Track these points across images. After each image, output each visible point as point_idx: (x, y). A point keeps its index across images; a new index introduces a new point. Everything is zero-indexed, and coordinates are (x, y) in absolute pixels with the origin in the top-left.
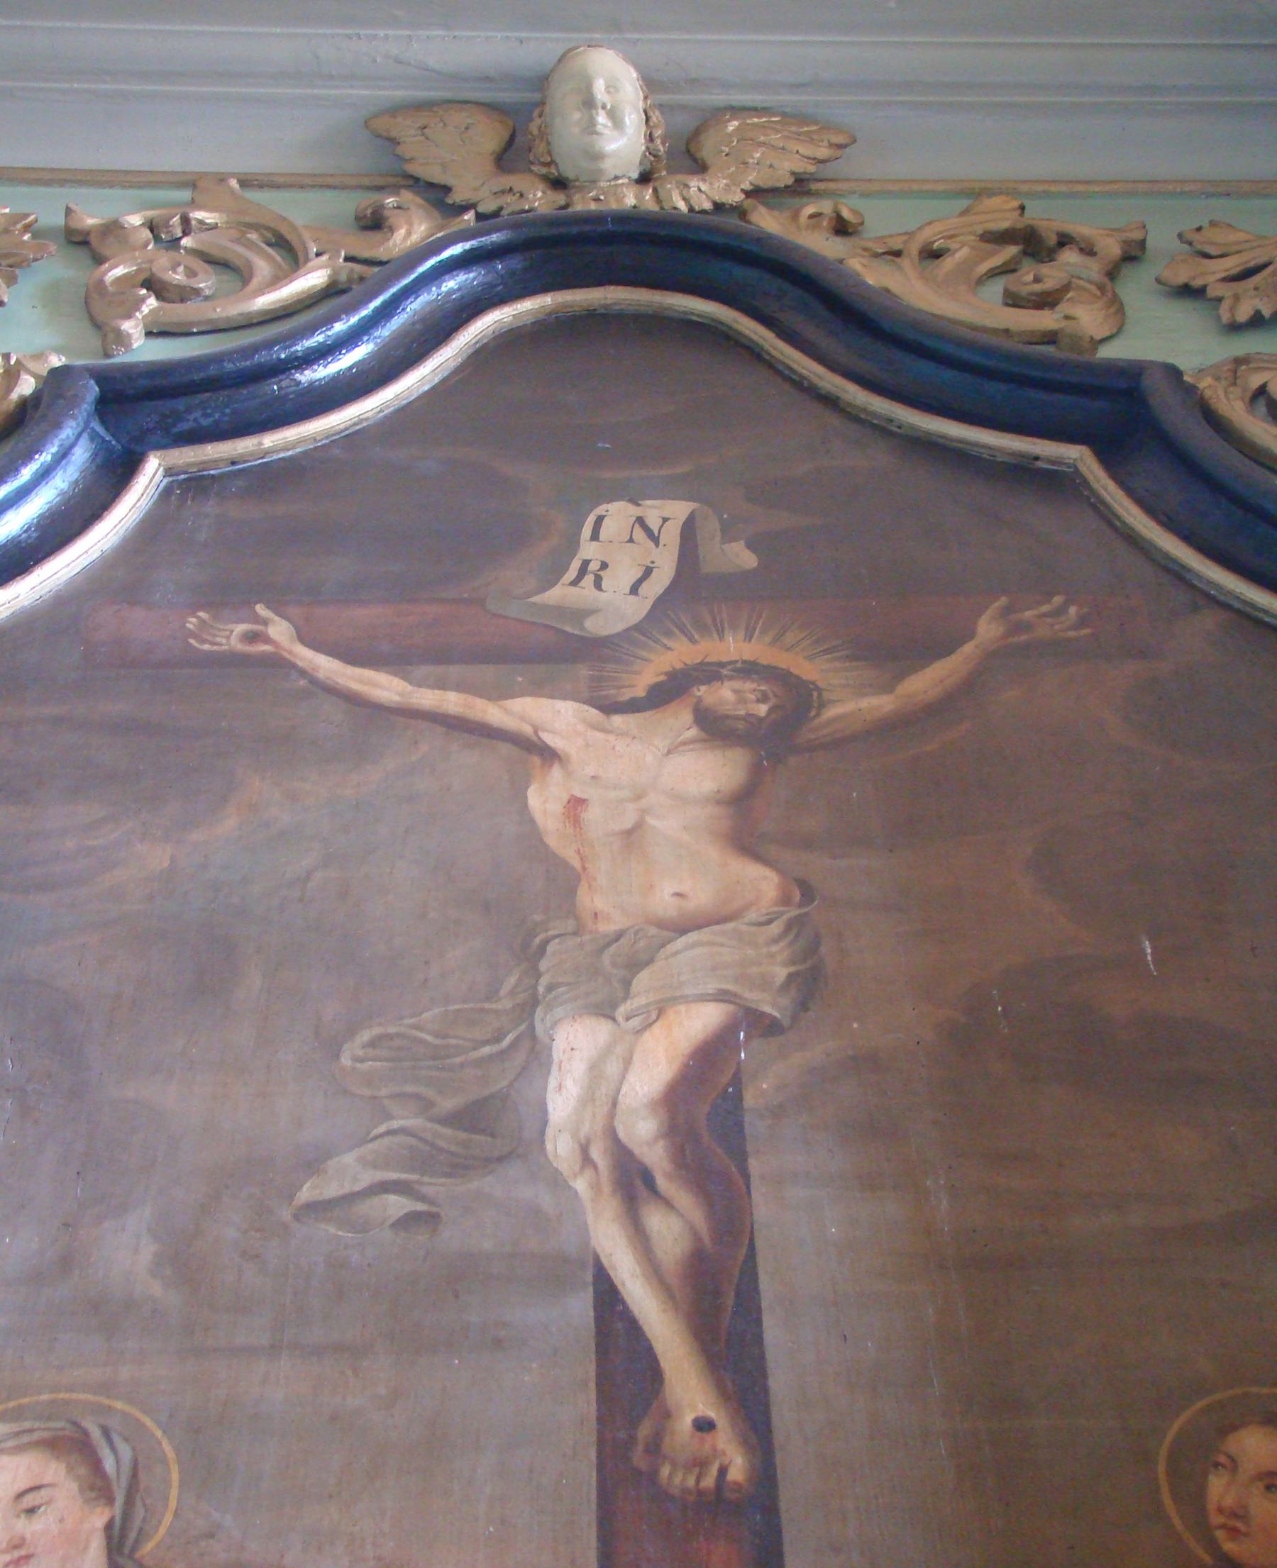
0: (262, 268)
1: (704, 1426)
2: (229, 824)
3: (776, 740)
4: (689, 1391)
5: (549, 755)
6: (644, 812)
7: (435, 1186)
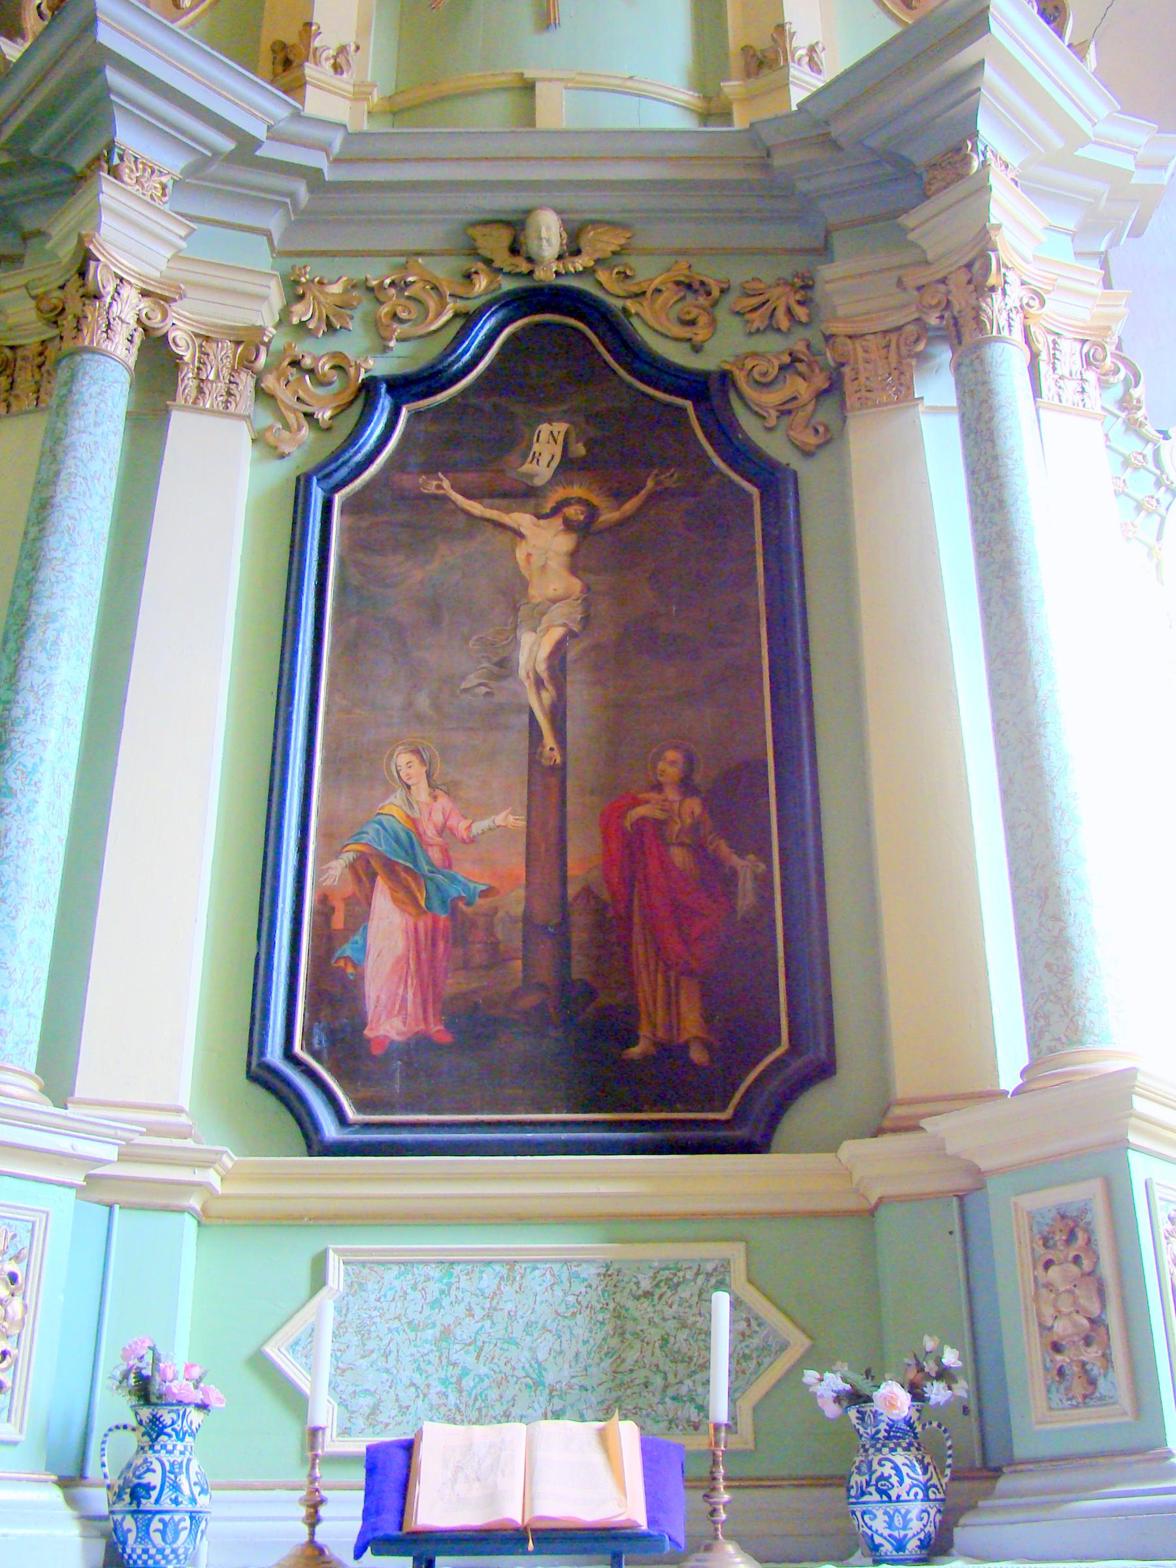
0: (432, 304)
1: (552, 749)
2: (436, 565)
3: (584, 529)
4: (549, 741)
5: (521, 536)
6: (547, 559)
7: (493, 684)
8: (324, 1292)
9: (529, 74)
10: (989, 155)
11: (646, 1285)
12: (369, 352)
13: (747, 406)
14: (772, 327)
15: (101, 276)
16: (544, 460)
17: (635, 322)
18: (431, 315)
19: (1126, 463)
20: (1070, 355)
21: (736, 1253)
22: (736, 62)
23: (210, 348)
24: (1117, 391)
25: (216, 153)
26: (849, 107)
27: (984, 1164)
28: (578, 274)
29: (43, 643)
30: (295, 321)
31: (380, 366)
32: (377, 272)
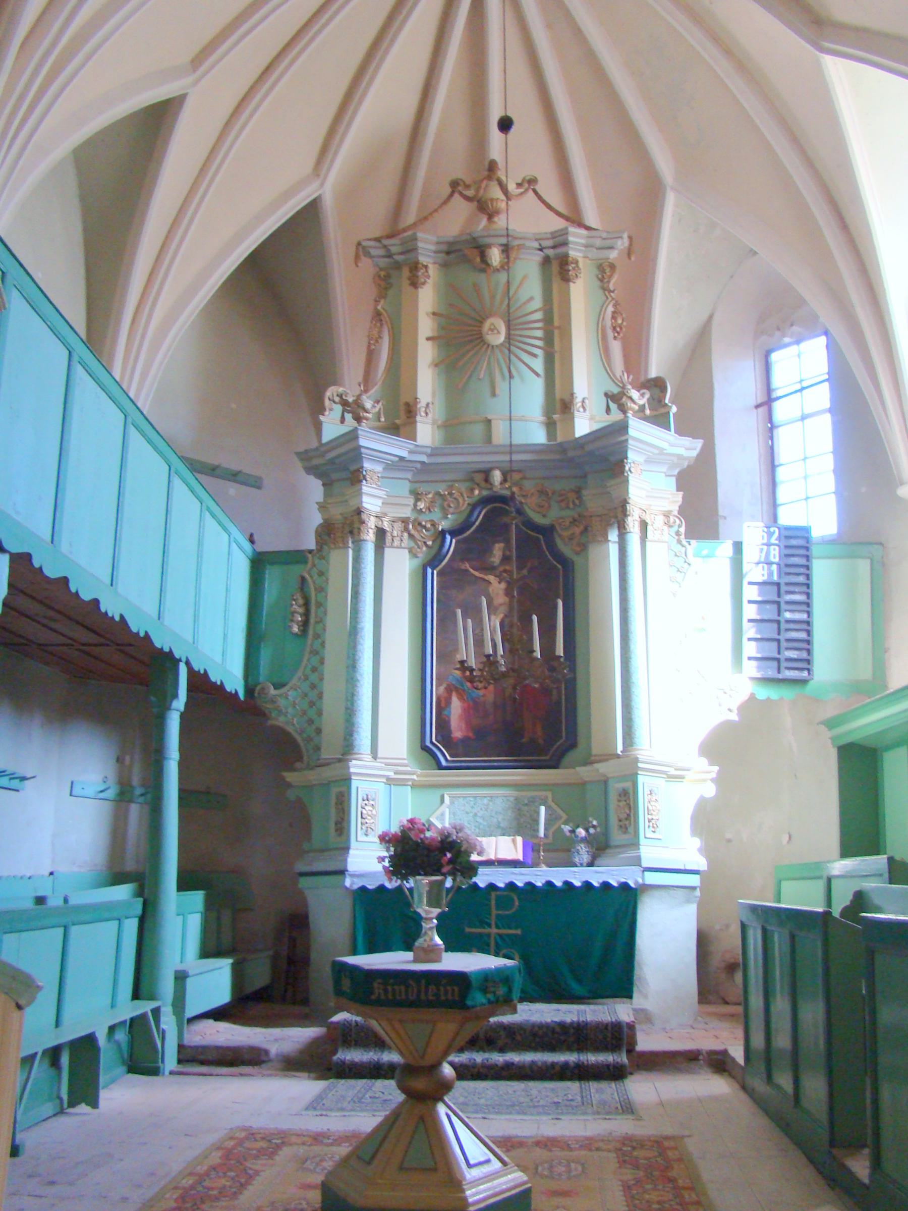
8: (444, 805)
9: (489, 418)
11: (526, 802)
14: (568, 507)
15: (364, 516)
17: (526, 508)
20: (661, 519)
21: (549, 794)
22: (558, 405)
23: (395, 525)
24: (675, 528)
26: (593, 441)
27: (609, 775)
32: (442, 489)
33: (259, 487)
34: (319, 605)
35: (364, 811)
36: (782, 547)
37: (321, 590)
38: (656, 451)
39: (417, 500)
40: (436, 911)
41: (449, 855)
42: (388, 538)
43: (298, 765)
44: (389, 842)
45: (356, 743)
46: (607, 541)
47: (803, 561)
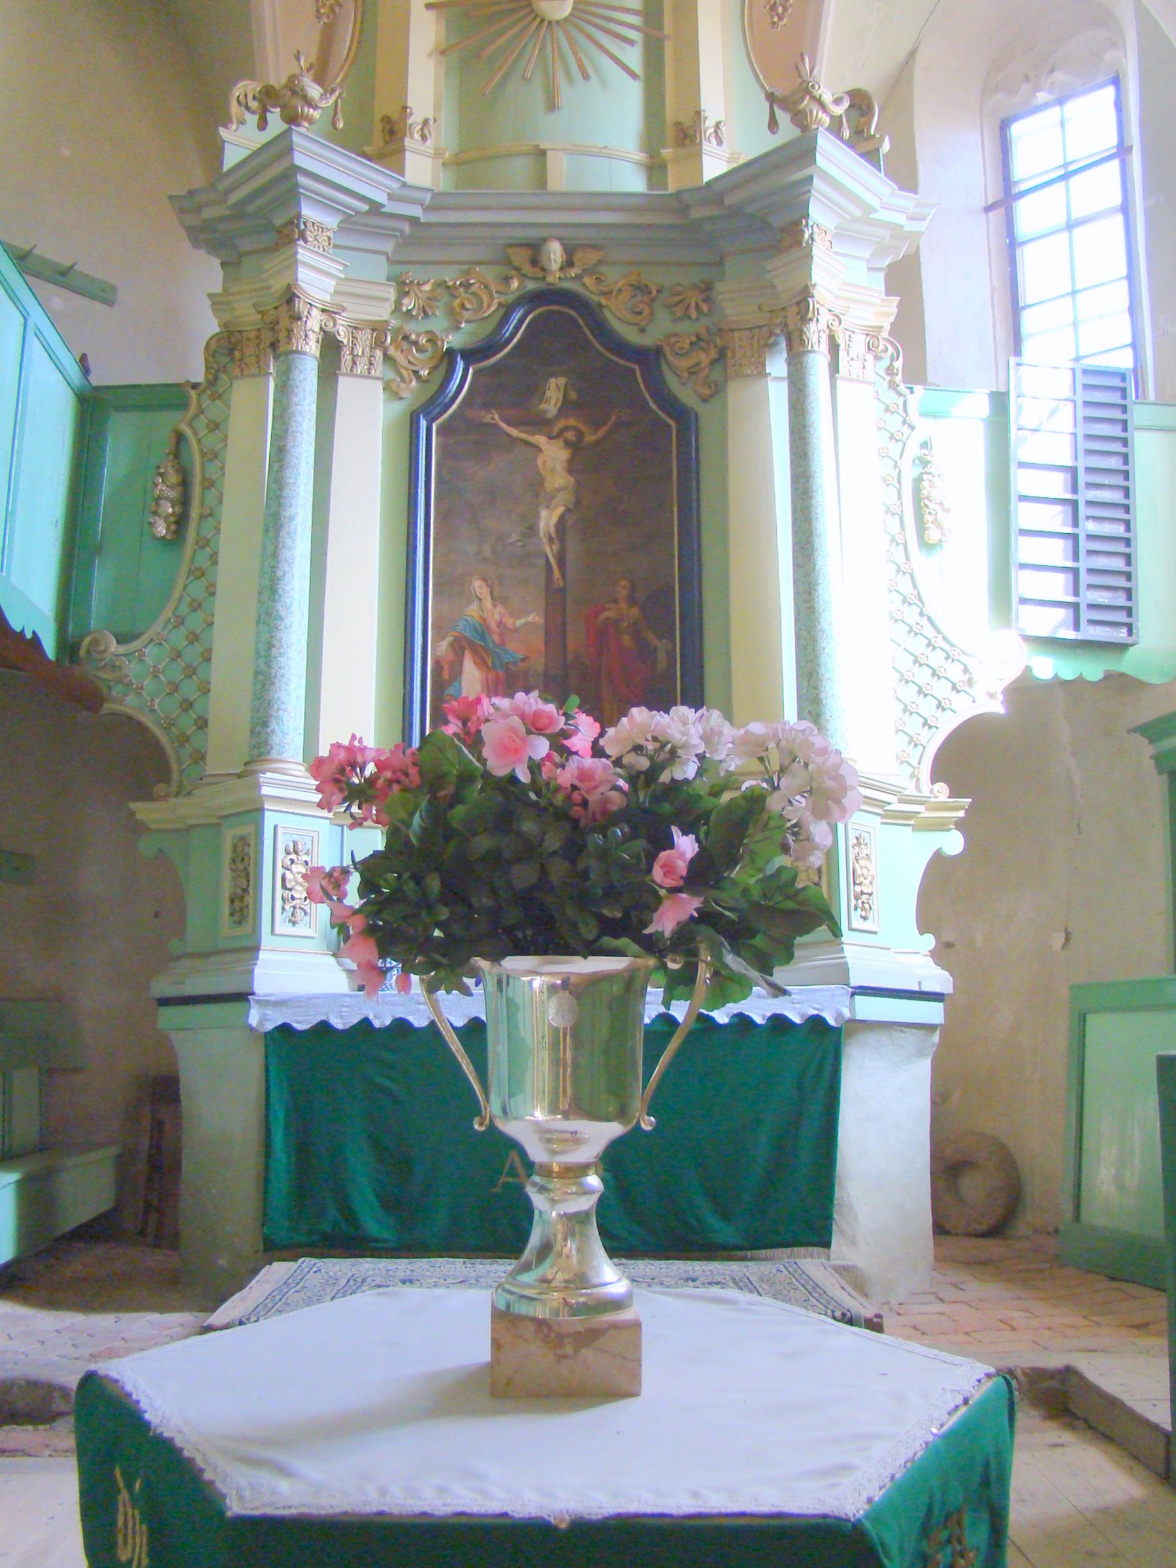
3: (575, 447)
4: (557, 574)
5: (541, 450)
9: (543, 146)
10: (815, 229)
12: (448, 331)
13: (669, 366)
15: (300, 306)
16: (553, 402)
18: (485, 305)
19: (887, 409)
20: (860, 341)
22: (670, 133)
23: (359, 334)
24: (886, 362)
25: (357, 213)
28: (572, 279)
29: (289, 533)
30: (404, 309)
31: (453, 340)
32: (450, 276)
33: (110, 303)
34: (208, 484)
35: (289, 875)
36: (1079, 403)
37: (212, 456)
38: (858, 213)
39: (403, 294)
40: (601, 1134)
41: (686, 845)
42: (346, 358)
43: (160, 789)
44: (362, 794)
45: (275, 740)
46: (762, 374)
47: (1116, 431)
